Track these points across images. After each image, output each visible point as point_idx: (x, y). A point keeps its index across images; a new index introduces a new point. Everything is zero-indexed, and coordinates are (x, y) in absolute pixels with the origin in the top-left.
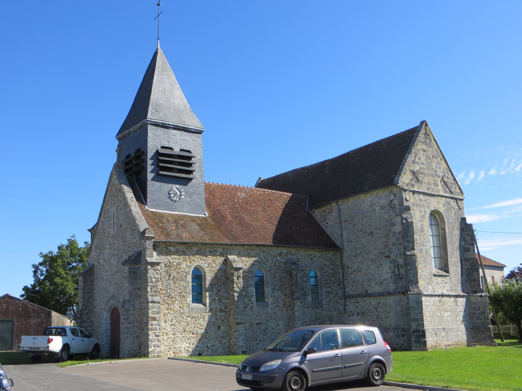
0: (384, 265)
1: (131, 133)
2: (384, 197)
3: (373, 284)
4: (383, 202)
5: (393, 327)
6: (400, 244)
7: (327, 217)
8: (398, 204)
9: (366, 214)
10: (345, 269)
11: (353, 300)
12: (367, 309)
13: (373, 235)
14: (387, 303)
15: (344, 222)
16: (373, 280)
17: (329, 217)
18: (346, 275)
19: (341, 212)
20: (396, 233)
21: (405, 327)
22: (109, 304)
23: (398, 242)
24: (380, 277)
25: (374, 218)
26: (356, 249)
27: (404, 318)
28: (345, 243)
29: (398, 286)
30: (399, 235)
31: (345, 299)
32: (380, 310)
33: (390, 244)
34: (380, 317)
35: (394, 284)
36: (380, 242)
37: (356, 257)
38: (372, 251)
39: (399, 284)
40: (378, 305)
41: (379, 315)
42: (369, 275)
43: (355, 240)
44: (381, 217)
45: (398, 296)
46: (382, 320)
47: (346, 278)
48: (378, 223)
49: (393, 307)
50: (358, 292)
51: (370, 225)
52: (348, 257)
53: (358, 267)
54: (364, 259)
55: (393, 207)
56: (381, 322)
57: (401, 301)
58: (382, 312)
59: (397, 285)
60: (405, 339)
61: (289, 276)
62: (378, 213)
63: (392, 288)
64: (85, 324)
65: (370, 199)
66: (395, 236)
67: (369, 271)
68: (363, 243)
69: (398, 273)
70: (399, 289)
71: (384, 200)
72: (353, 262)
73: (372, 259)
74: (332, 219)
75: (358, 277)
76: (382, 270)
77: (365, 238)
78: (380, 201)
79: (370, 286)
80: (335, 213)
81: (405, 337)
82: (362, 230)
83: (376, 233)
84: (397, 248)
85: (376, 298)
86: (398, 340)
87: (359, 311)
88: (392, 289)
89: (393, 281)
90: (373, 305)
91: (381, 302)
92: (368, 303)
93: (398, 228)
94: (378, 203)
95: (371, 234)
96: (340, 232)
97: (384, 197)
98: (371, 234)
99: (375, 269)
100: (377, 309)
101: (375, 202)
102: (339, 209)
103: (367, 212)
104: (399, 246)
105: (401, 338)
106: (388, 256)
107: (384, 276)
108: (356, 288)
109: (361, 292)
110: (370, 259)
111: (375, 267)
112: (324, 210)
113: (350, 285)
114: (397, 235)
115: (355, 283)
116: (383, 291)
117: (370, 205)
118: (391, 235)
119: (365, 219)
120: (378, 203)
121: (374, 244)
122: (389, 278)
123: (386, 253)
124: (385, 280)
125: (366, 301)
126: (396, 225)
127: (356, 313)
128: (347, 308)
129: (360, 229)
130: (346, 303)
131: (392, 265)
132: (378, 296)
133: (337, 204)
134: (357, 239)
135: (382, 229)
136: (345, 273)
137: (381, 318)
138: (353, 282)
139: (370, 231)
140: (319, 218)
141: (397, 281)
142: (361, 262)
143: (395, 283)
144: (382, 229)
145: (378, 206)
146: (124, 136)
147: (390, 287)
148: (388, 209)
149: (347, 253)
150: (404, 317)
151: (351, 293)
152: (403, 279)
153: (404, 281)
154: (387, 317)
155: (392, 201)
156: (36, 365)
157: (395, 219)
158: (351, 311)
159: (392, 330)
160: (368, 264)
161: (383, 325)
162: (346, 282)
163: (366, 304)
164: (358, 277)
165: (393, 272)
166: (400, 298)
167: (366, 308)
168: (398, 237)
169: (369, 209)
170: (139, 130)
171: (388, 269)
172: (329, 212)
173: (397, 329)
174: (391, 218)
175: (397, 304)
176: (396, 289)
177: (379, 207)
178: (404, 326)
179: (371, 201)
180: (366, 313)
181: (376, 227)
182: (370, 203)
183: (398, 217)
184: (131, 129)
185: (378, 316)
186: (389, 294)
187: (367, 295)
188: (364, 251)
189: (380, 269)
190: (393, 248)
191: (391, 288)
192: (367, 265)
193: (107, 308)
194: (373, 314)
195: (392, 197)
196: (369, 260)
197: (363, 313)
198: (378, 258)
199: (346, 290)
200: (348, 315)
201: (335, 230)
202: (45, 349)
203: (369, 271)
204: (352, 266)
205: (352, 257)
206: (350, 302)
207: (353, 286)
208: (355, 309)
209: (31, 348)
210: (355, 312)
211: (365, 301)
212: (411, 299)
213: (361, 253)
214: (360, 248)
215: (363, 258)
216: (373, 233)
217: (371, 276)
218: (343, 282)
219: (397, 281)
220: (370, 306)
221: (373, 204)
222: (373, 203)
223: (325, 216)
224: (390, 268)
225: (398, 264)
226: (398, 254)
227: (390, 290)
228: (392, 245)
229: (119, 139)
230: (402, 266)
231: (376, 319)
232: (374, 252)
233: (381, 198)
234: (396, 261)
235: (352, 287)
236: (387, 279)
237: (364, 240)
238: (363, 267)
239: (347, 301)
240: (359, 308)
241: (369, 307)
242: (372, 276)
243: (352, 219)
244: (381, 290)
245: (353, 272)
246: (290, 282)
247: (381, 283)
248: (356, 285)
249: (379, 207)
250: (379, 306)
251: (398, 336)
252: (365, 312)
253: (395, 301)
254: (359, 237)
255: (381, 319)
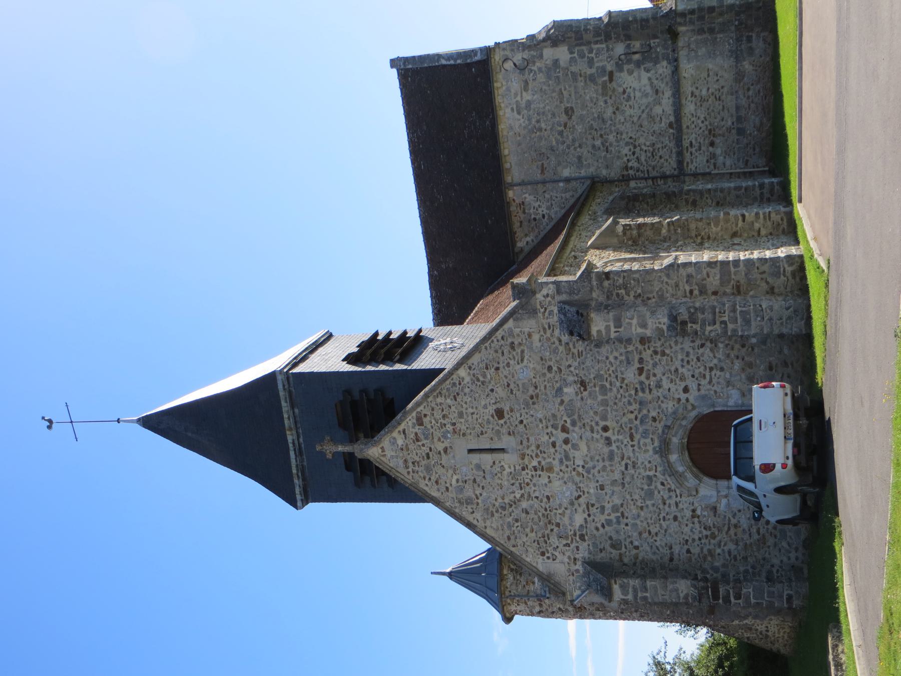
0: (625, 86)
1: (298, 440)
2: (507, 82)
3: (658, 110)
4: (515, 85)
5: (735, 63)
6: (591, 51)
7: (533, 216)
8: (521, 54)
9: (534, 121)
10: (629, 174)
11: (687, 156)
12: (703, 122)
13: (572, 108)
14: (692, 75)
15: (544, 174)
16: (651, 109)
17: (532, 211)
18: (640, 172)
19: (526, 180)
20: (571, 58)
21: (735, 37)
22: (681, 469)
23: (587, 55)
24: (646, 95)
25: (542, 106)
26: (594, 146)
27: (718, 40)
28: (583, 173)
29: (663, 54)
30: (574, 53)
31: (685, 175)
32: (704, 92)
33: (589, 72)
34: (718, 92)
35: (659, 63)
36: (585, 93)
37: (610, 148)
38: (600, 110)
39: (659, 52)
40: (696, 96)
41: (713, 94)
42: (642, 118)
43: (578, 149)
44: (542, 89)
45: (681, 53)
46: (723, 87)
47: (646, 172)
48: (552, 97)
49: (698, 63)
50: (672, 145)
51: (554, 115)
52: (607, 167)
53: (627, 144)
54: (613, 128)
55: (526, 63)
56: (725, 90)
57: (689, 45)
58: (708, 89)
59: (660, 57)
60: (754, 35)
61: (637, 204)
62: (534, 95)
63: (666, 67)
64: (731, 576)
65: (508, 110)
66: (576, 61)
67: (635, 119)
68: (584, 130)
69: (640, 54)
70: (668, 52)
71: (512, 81)
72: (617, 154)
73: (614, 113)
74: (536, 205)
75: (645, 144)
76: (634, 89)
77: (576, 126)
78: (513, 91)
79: (661, 118)
80: (527, 195)
81: (751, 36)
82: (561, 133)
83: (568, 102)
84: (596, 57)
85: (683, 102)
86: (757, 51)
87: (707, 142)
88: (668, 68)
89: (653, 65)
90: (696, 110)
91: (690, 89)
92: (692, 119)
93: (562, 53)
94: (516, 95)
95: (570, 113)
96: (561, 184)
97: (507, 82)
98: (569, 112)
99: (632, 105)
100: (702, 100)
101: (515, 100)
102: (520, 184)
103: (529, 120)
104: (594, 51)
105: (754, 44)
106: (609, 75)
107: (645, 86)
108: (665, 150)
109: (672, 138)
110: (613, 116)
111: (628, 106)
112: (519, 224)
113: (659, 163)
114: (575, 57)
115: (656, 151)
116: (671, 87)
117: (519, 113)
118: (573, 69)
119: (543, 125)
120: (516, 95)
121: (587, 106)
122: (649, 75)
123: (604, 81)
124: (651, 84)
125: (689, 124)
126: (556, 58)
127: (711, 149)
128: (702, 171)
129: (559, 137)
130: (692, 172)
131: (626, 67)
132: (679, 95)
133: (512, 185)
134: (577, 144)
135: (563, 88)
136: (637, 174)
137: (719, 91)
138: (653, 157)
139: (564, 115)
140: (532, 237)
141: (654, 56)
142: (618, 136)
143: (656, 61)
144: (563, 88)
145: (522, 96)
146: (300, 474)
147: (664, 72)
148: (529, 74)
149: (599, 168)
150: (716, 38)
151: (673, 163)
152: (650, 43)
153: (654, 43)
154: (717, 75)
155: (515, 64)
156: (835, 447)
157: (546, 60)
158: (707, 161)
159: (739, 65)
160: (622, 120)
161: (731, 86)
162: (654, 174)
163: (693, 126)
164: (645, 144)
165: (638, 64)
166: (683, 47)
167: (701, 125)
168: (578, 55)
169: (525, 116)
170: (296, 411)
171: (632, 76)
172: (524, 212)
173: (738, 52)
174: (544, 69)
175: (693, 54)
176: (668, 59)
177: (524, 94)
178: (732, 38)
179: (512, 109)
180: (710, 124)
181: (557, 101)
182: (515, 112)
183: (544, 53)
184: (290, 439)
185: (716, 97)
186: (676, 71)
187: (677, 124)
188: (598, 129)
189: (632, 95)
190: (597, 65)
191: (665, 70)
192: (623, 123)
193: (691, 481)
194: (712, 108)
195: (509, 65)
196: (615, 119)
197: (710, 131)
198: (613, 98)
199: (668, 173)
200: (715, 168)
201: (557, 197)
202: (786, 394)
203: (635, 119)
204: (625, 159)
205: (608, 156)
206: (690, 164)
207: (661, 157)
208: (704, 152)
209: (785, 437)
210: (708, 151)
211: (688, 127)
212: (685, 6)
213: (601, 136)
214: (593, 139)
215: (611, 131)
216: (568, 107)
217: (644, 115)
218: (653, 179)
219: (654, 56)
220: (698, 115)
221: (517, 107)
222: (515, 107)
223: (529, 221)
224: (630, 72)
225: (625, 54)
226: (606, 55)
227: (670, 72)
228: (591, 68)
229: (305, 502)
230: (628, 46)
231: (721, 102)
232: (601, 106)
233: (508, 89)
234: (620, 59)
235: (662, 160)
236: (650, 79)
237: (579, 128)
238: (627, 133)
239: (689, 172)
240: (702, 141)
241: (699, 118)
242: (643, 112)
243: (540, 154)
244: (668, 93)
245: (636, 156)
246: (647, 203)
247: (657, 92)
248: (659, 148)
249: (523, 92)
250: (697, 94)
251: (751, 51)
252: (709, 127)
253: (688, 60)
254: (574, 140)
255: (721, 91)
